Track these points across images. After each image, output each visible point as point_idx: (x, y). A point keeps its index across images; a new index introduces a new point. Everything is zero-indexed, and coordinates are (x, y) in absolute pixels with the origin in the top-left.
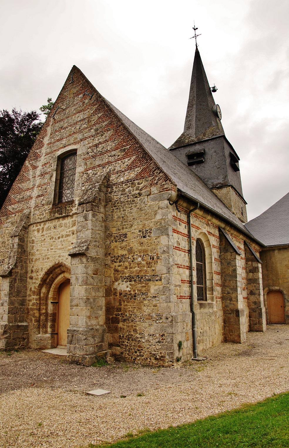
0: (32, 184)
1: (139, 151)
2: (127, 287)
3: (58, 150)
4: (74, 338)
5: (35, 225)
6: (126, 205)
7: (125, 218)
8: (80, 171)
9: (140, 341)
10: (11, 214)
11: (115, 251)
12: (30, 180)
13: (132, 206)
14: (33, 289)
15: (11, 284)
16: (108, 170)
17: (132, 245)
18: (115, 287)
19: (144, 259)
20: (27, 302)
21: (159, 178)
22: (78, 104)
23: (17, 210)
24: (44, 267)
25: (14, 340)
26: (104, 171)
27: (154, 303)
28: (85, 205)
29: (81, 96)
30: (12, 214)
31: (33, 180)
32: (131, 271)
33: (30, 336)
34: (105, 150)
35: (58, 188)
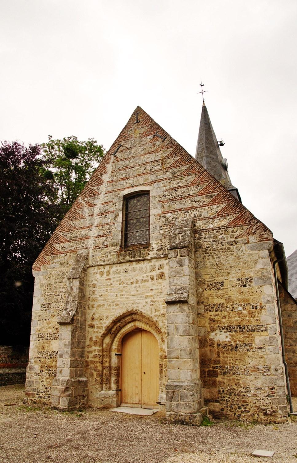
0: (88, 223)
1: (230, 198)
2: (227, 337)
3: (124, 189)
4: (176, 394)
5: (96, 268)
6: (220, 253)
7: (220, 265)
8: (156, 213)
9: (245, 396)
10: (60, 254)
11: (210, 300)
12: (85, 218)
13: (227, 254)
14: (94, 339)
15: (72, 333)
16: (193, 216)
17: (230, 294)
18: (212, 338)
19: (245, 309)
20: (86, 353)
21: (257, 228)
22: (148, 144)
23: (69, 249)
24: (110, 314)
25: (75, 399)
26: (188, 216)
27: (260, 354)
28: (178, 250)
29: (151, 137)
30: (62, 254)
31: (90, 218)
32: (231, 321)
33: (90, 393)
34: (187, 194)
35: (124, 229)
